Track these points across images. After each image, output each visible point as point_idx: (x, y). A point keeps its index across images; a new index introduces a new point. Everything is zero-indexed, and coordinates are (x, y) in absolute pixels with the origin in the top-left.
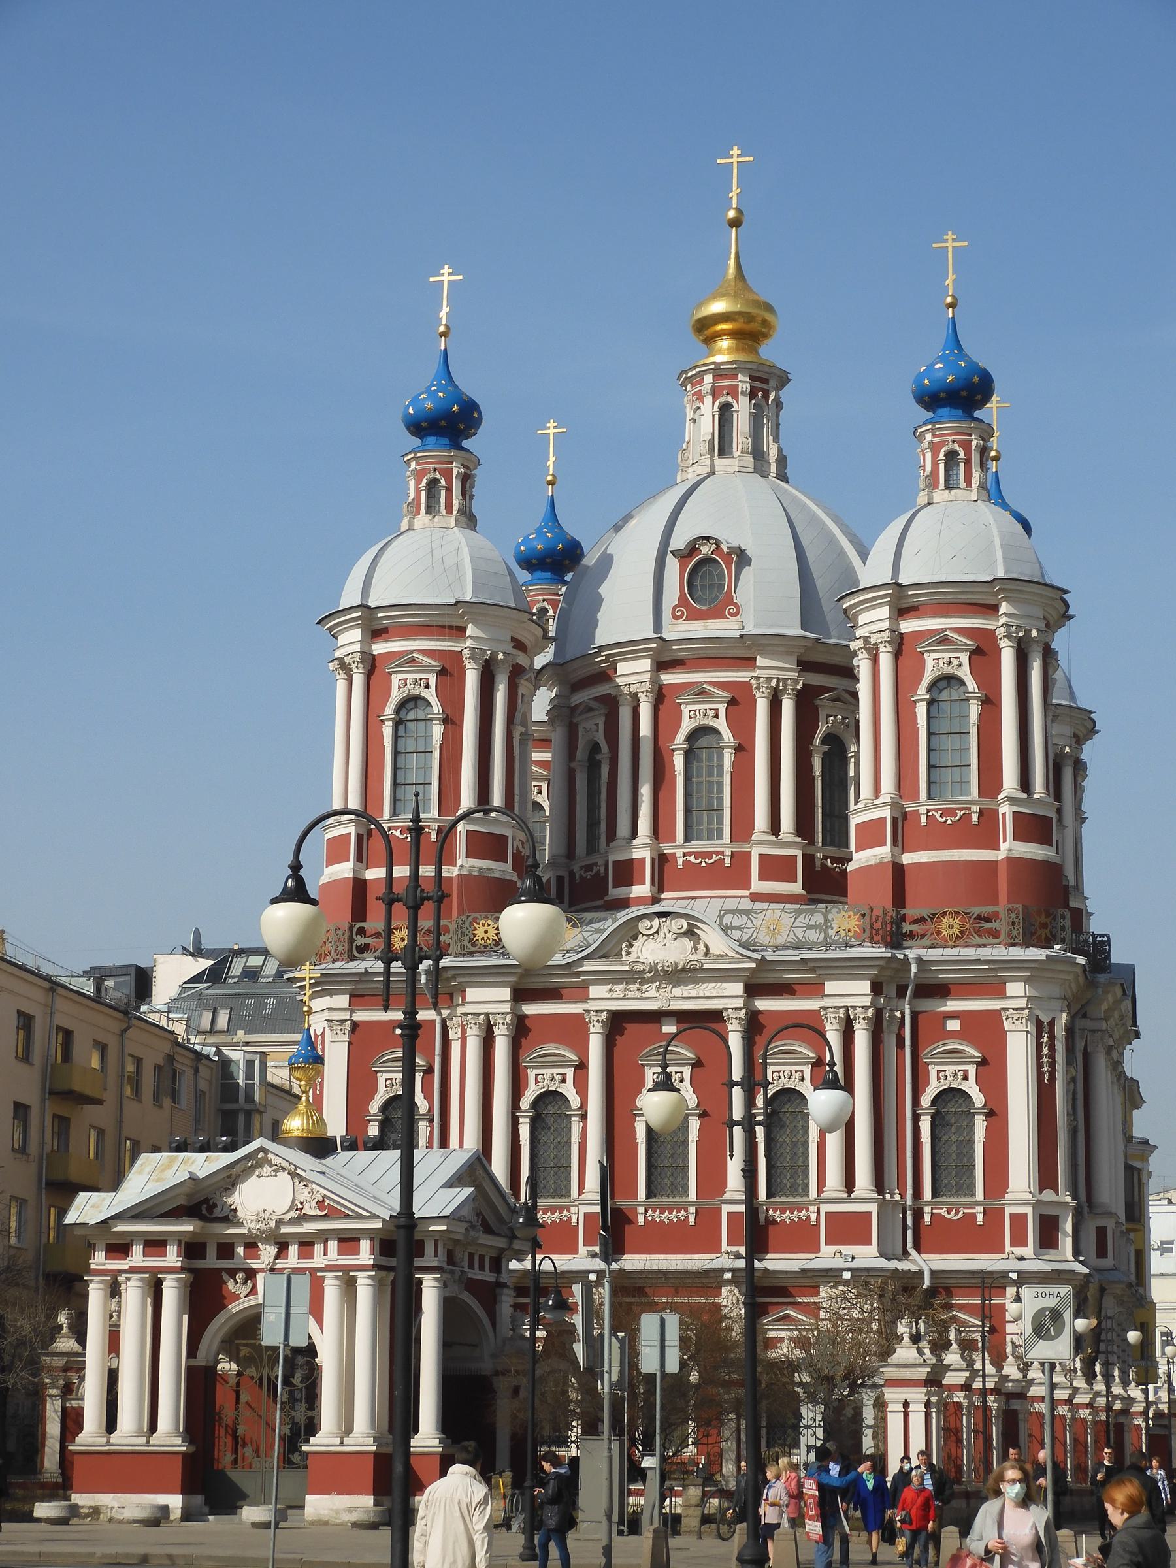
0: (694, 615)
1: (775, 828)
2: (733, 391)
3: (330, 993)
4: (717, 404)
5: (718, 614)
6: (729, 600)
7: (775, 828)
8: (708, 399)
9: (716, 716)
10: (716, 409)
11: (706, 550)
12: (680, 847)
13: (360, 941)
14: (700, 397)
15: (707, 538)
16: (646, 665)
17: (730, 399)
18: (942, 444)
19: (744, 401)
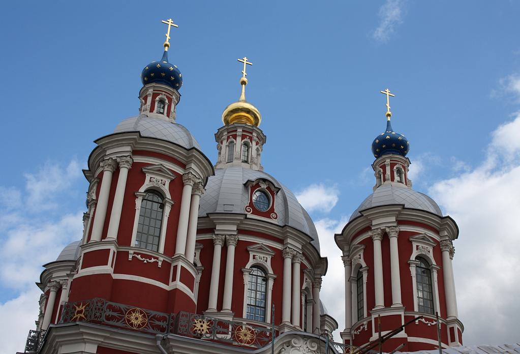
0: (256, 212)
1: (291, 322)
2: (251, 139)
3: (84, 341)
4: (243, 141)
5: (267, 214)
6: (272, 210)
7: (291, 322)
8: (239, 139)
9: (266, 261)
10: (242, 143)
11: (264, 186)
12: (245, 320)
13: (110, 313)
14: (235, 137)
15: (264, 180)
16: (234, 228)
17: (249, 141)
18: (396, 164)
19: (254, 143)
